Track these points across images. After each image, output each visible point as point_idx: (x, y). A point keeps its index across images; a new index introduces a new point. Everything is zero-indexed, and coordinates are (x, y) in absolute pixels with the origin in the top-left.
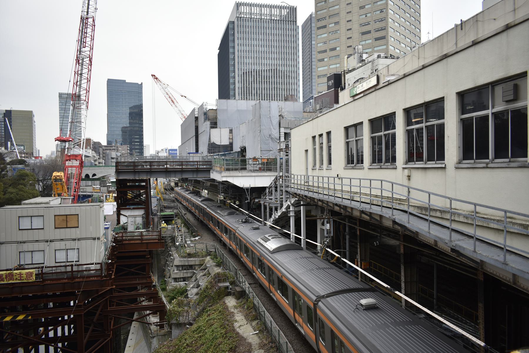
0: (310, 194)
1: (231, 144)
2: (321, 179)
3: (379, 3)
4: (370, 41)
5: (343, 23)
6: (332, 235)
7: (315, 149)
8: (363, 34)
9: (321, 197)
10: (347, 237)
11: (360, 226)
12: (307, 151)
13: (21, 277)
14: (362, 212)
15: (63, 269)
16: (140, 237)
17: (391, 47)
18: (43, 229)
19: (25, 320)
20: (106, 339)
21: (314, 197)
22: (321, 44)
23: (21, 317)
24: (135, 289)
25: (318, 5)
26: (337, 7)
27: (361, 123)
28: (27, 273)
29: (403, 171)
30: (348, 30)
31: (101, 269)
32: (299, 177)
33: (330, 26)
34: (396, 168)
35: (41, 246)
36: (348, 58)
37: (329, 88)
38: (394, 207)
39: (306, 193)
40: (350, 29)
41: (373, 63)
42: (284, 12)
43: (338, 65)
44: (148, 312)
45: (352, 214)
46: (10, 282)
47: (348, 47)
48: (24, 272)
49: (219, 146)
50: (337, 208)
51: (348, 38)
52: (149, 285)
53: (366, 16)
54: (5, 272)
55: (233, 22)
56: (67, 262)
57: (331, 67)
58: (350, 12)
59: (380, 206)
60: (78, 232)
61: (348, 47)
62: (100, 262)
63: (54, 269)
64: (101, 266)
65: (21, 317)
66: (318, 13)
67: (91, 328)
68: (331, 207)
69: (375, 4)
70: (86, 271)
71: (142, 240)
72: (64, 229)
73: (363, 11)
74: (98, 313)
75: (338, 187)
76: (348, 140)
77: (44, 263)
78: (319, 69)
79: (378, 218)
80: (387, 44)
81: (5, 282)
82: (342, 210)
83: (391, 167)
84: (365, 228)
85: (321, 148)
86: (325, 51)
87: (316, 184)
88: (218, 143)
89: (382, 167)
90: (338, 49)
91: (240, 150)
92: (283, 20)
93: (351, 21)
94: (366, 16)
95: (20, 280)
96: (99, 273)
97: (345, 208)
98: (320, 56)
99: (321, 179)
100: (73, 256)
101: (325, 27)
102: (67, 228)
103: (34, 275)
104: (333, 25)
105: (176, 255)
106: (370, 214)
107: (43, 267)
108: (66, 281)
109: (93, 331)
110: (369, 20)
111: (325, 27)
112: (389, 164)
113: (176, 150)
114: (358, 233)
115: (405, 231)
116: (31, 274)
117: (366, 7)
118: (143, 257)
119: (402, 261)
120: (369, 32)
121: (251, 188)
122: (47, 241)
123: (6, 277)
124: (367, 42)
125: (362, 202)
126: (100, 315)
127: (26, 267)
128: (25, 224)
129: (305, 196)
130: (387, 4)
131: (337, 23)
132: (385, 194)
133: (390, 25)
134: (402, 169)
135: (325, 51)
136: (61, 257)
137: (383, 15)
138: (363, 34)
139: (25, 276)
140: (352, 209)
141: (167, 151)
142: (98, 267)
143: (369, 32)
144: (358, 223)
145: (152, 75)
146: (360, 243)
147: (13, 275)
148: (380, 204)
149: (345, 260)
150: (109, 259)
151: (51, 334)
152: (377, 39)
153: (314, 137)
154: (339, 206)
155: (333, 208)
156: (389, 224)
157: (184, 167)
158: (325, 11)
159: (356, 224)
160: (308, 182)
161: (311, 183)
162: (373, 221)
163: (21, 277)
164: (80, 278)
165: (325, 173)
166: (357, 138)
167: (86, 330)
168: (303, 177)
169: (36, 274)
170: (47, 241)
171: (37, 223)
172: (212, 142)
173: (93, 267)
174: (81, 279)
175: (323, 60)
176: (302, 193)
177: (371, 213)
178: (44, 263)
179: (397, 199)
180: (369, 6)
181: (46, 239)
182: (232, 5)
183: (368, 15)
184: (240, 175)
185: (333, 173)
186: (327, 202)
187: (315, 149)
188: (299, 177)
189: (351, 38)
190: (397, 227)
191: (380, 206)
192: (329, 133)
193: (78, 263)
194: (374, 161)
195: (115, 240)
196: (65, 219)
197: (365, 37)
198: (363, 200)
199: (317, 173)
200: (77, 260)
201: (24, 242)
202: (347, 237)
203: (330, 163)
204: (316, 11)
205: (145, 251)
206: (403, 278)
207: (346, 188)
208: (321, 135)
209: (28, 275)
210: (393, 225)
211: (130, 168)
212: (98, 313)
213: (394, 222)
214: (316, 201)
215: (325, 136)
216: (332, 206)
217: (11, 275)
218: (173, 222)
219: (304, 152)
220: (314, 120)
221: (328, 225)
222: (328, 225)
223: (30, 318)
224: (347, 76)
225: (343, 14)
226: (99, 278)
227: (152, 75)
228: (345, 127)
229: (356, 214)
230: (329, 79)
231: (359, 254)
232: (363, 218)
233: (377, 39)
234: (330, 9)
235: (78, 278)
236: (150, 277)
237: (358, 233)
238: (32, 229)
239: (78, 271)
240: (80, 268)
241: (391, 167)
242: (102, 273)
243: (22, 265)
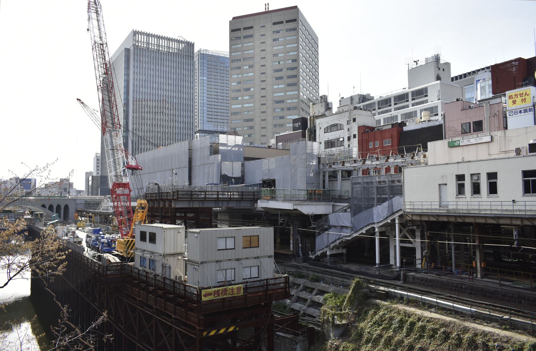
1: (243, 176)
3: (291, 53)
4: (283, 86)
5: (257, 67)
8: (277, 78)
13: (233, 292)
15: (258, 284)
17: (301, 94)
18: (234, 249)
22: (235, 84)
23: (231, 329)
25: (233, 47)
26: (252, 51)
28: (238, 288)
30: (262, 74)
33: (245, 67)
35: (234, 264)
36: (314, 104)
37: (295, 129)
40: (264, 73)
41: (350, 113)
42: (181, 46)
43: (252, 105)
46: (225, 297)
47: (262, 89)
48: (235, 287)
49: (232, 178)
51: (262, 81)
53: (279, 63)
55: (127, 50)
56: (251, 278)
57: (245, 105)
58: (264, 58)
60: (259, 251)
61: (262, 89)
63: (252, 283)
65: (231, 329)
66: (233, 54)
69: (288, 54)
72: (248, 249)
73: (275, 58)
77: (234, 280)
78: (233, 107)
80: (298, 90)
81: (221, 297)
86: (239, 91)
88: (230, 175)
90: (252, 89)
91: (261, 182)
92: (179, 54)
93: (264, 65)
94: (279, 63)
95: (233, 294)
98: (234, 95)
100: (255, 274)
101: (239, 68)
102: (251, 247)
103: (242, 289)
104: (247, 67)
110: (281, 67)
111: (239, 68)
113: (30, 180)
116: (240, 288)
117: (280, 55)
120: (281, 78)
121: (315, 215)
122: (238, 260)
123: (222, 293)
124: (280, 86)
127: (233, 282)
128: (221, 244)
130: (298, 55)
131: (251, 67)
133: (301, 74)
135: (239, 91)
136: (246, 274)
137: (295, 64)
138: (277, 78)
139: (236, 291)
141: (18, 181)
143: (281, 78)
145: (78, 99)
152: (289, 85)
157: (232, 197)
158: (240, 53)
163: (233, 292)
169: (244, 288)
170: (217, 261)
171: (230, 244)
172: (223, 173)
175: (237, 98)
178: (234, 280)
180: (282, 55)
181: (237, 258)
182: (127, 32)
183: (281, 63)
189: (264, 81)
193: (258, 279)
196: (249, 239)
197: (278, 81)
200: (257, 276)
201: (221, 261)
204: (231, 52)
209: (236, 290)
211: (187, 196)
217: (226, 290)
223: (238, 329)
224: (318, 121)
225: (257, 59)
226: (284, 290)
227: (78, 99)
230: (295, 121)
233: (289, 85)
234: (245, 52)
238: (226, 249)
243: (229, 281)
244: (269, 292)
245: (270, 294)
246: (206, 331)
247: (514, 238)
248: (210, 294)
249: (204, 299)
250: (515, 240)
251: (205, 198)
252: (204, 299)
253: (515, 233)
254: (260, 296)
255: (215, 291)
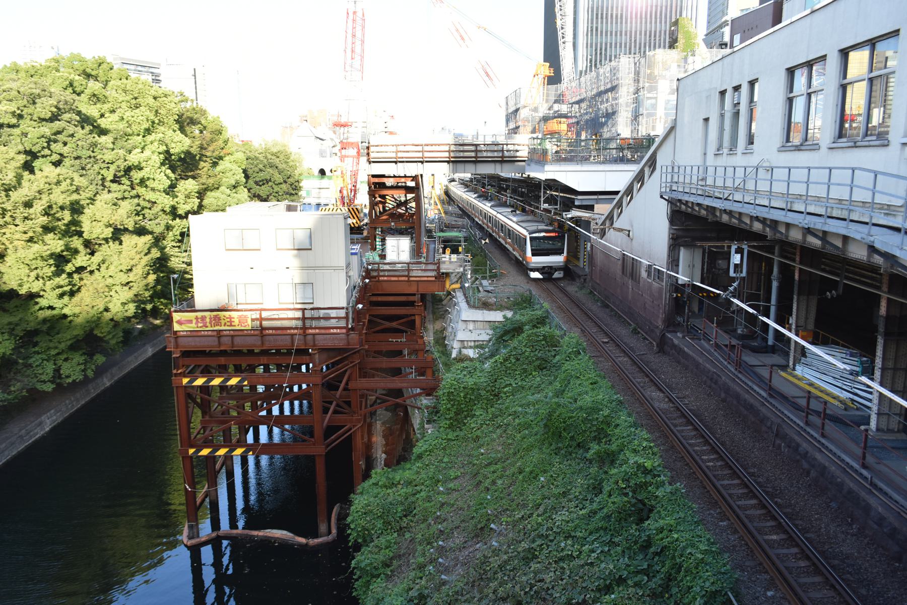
0: (707, 202)
2: (730, 171)
6: (744, 274)
7: (722, 116)
9: (728, 206)
10: (775, 284)
11: (801, 263)
12: (706, 120)
14: (808, 231)
16: (406, 273)
19: (239, 387)
20: (354, 426)
21: (714, 205)
24: (399, 353)
27: (823, 58)
29: (902, 150)
31: (347, 318)
32: (688, 169)
34: (888, 145)
38: (874, 221)
39: (700, 200)
44: (418, 391)
45: (787, 237)
46: (217, 328)
50: (757, 226)
52: (420, 350)
54: (209, 313)
59: (845, 220)
62: (345, 305)
64: (347, 314)
67: (332, 408)
68: (746, 224)
70: (324, 318)
71: (408, 276)
74: (342, 385)
75: (763, 186)
76: (791, 95)
79: (839, 243)
82: (768, 229)
83: (877, 143)
84: (811, 267)
85: (737, 114)
87: (719, 183)
89: (858, 144)
95: (231, 325)
96: (343, 323)
97: (775, 224)
99: (730, 171)
105: (463, 304)
106: (824, 236)
107: (261, 310)
108: (296, 331)
109: (335, 412)
112: (874, 138)
114: (797, 277)
115: (892, 267)
118: (412, 304)
119: (881, 329)
125: (809, 214)
126: (345, 389)
129: (699, 205)
132: (860, 195)
134: (899, 146)
140: (788, 226)
142: (342, 313)
144: (798, 259)
146: (799, 295)
147: (219, 319)
148: (844, 214)
149: (765, 319)
150: (358, 302)
151: (276, 411)
153: (723, 93)
154: (763, 221)
155: (751, 226)
156: (858, 253)
159: (794, 260)
160: (704, 179)
161: (710, 181)
162: (829, 249)
163: (231, 322)
164: (315, 328)
165: (739, 160)
166: (810, 91)
167: (326, 411)
168: (695, 169)
173: (333, 313)
174: (317, 331)
176: (692, 199)
177: (825, 233)
179: (882, 206)
184: (578, 167)
185: (754, 160)
186: (740, 214)
187: (722, 116)
188: (688, 169)
190: (878, 260)
191: (845, 220)
192: (752, 83)
194: (841, 134)
195: (368, 273)
198: (811, 209)
199: (724, 160)
202: (775, 284)
203: (751, 142)
205: (414, 295)
206: (878, 362)
207: (780, 188)
208: (737, 88)
210: (869, 256)
212: (342, 385)
213: (872, 249)
214: (718, 214)
215: (745, 89)
216: (748, 222)
217: (217, 318)
218: (460, 249)
219: (702, 121)
220: (725, 60)
221: (738, 256)
222: (738, 256)
223: (246, 383)
226: (344, 331)
228: (788, 69)
229: (795, 236)
231: (794, 316)
232: (809, 243)
235: (311, 328)
236: (422, 337)
237: (797, 277)
239: (312, 319)
240: (316, 314)
241: (877, 143)
242: (347, 324)
244: (310, 331)
245: (314, 335)
246: (185, 377)
247: (732, 273)
248: (190, 321)
249: (176, 327)
250: (733, 280)
251: (502, 157)
252: (176, 327)
253: (736, 259)
254: (292, 335)
255: (197, 318)
